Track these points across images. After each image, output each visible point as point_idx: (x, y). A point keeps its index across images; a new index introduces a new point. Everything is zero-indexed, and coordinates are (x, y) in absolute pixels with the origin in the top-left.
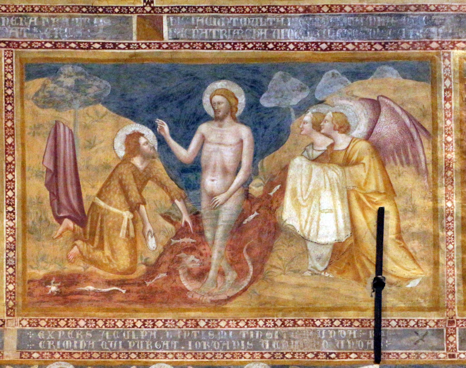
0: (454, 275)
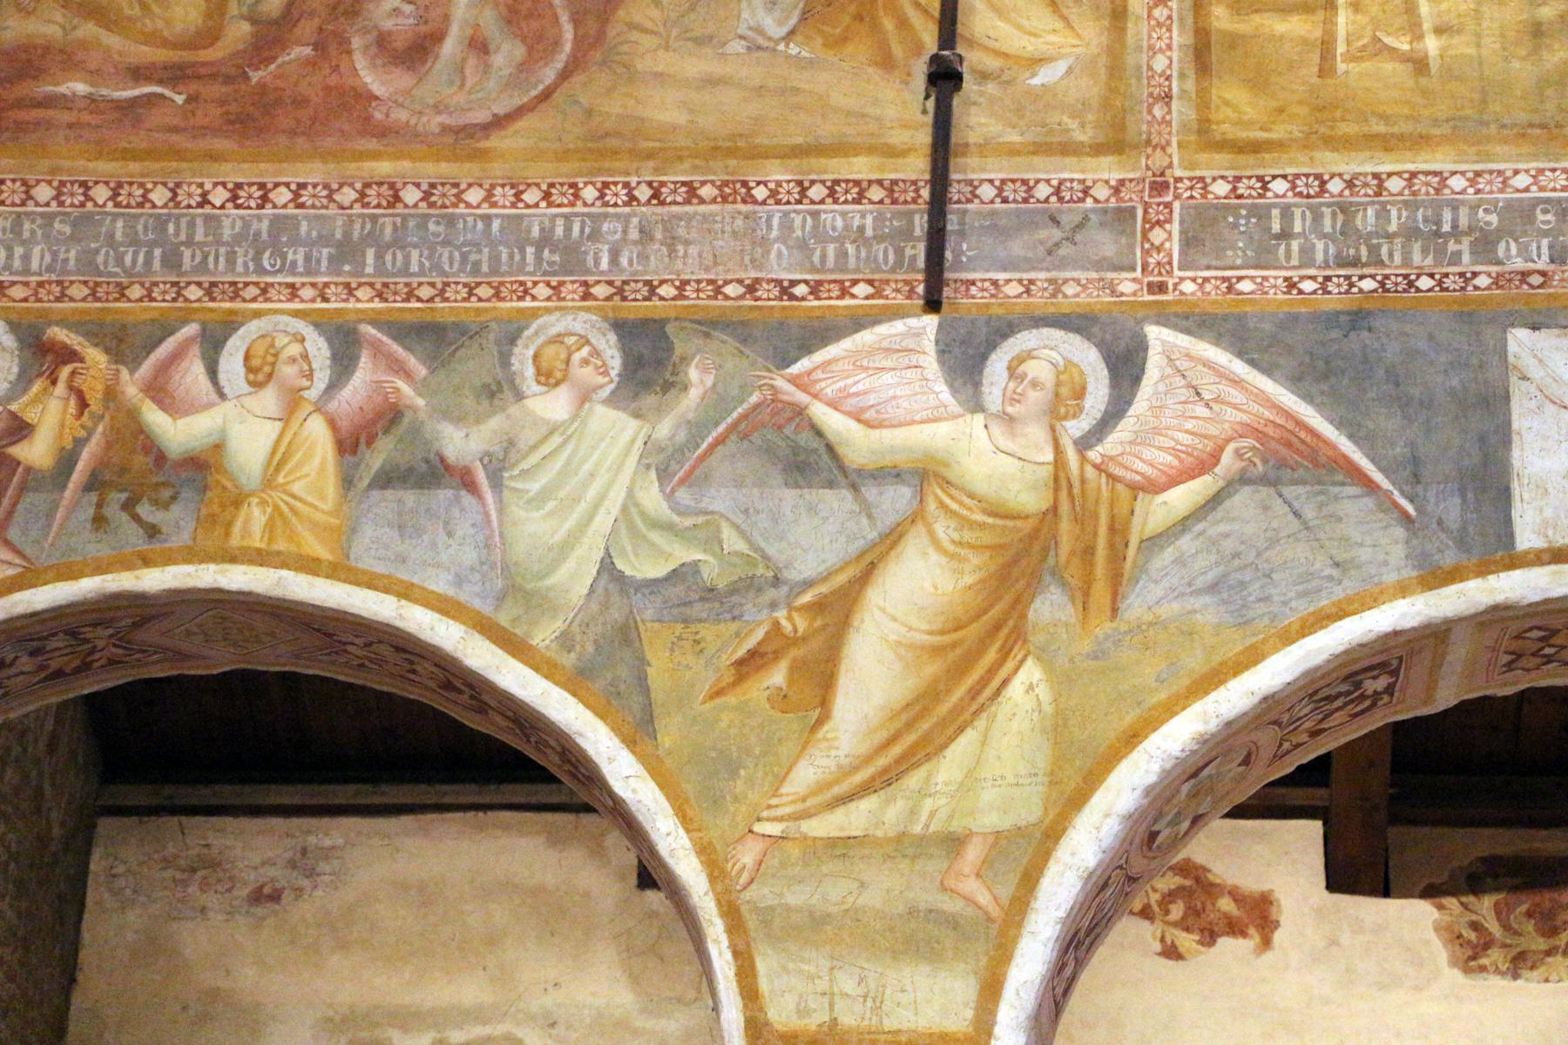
0: (1169, 47)
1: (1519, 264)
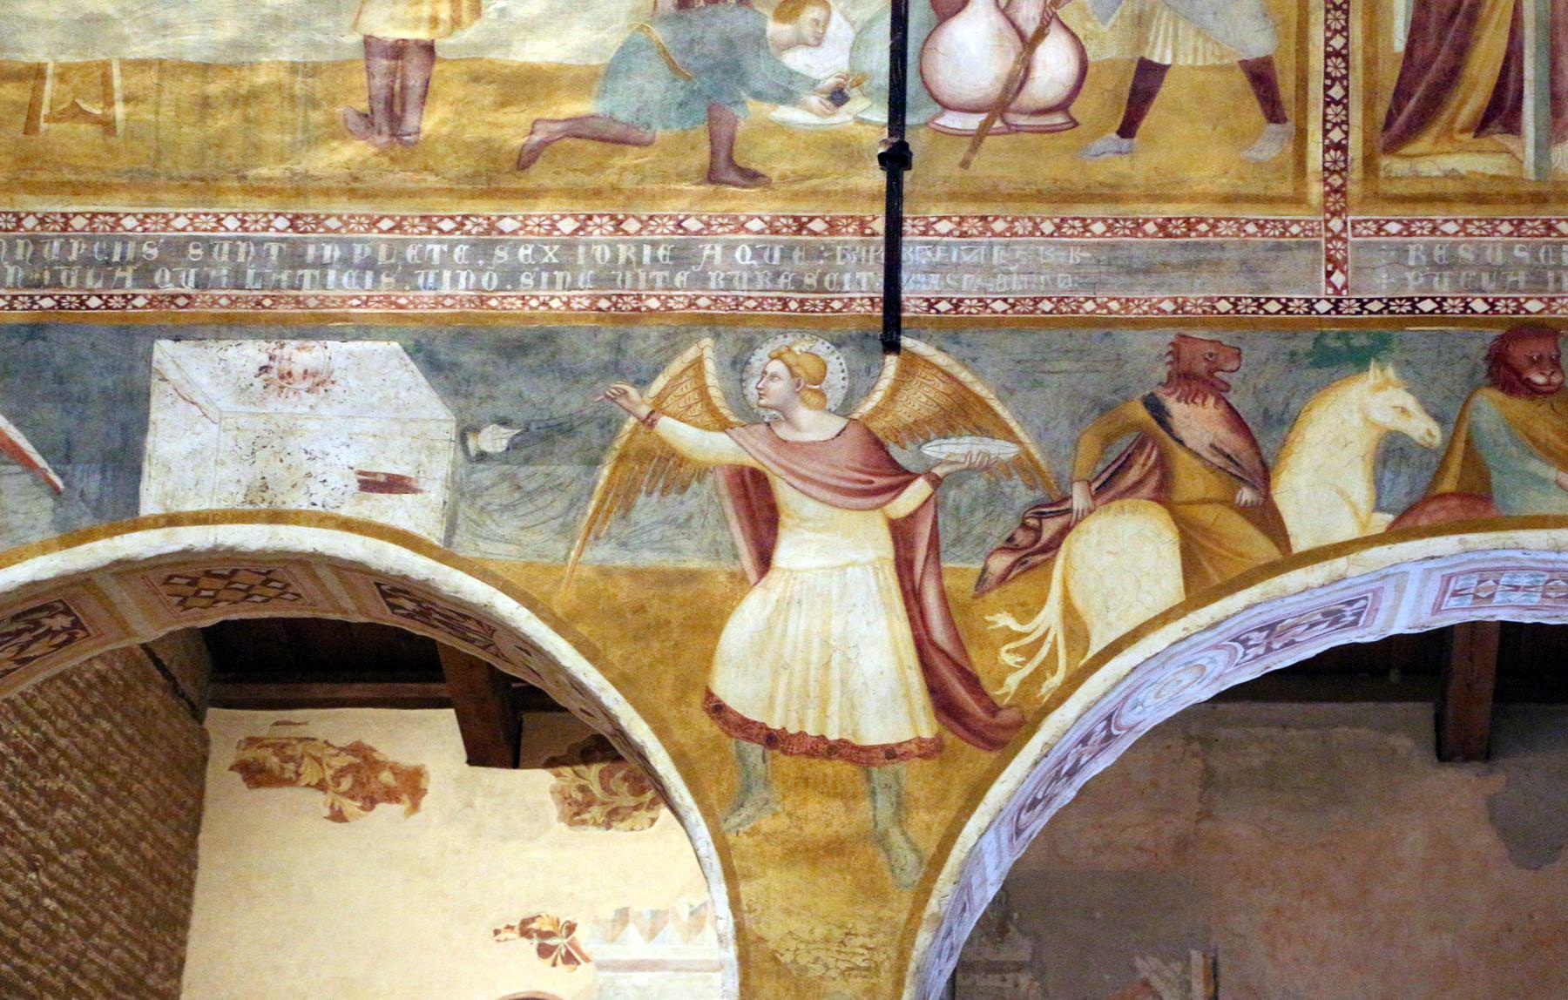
1: (170, 289)
